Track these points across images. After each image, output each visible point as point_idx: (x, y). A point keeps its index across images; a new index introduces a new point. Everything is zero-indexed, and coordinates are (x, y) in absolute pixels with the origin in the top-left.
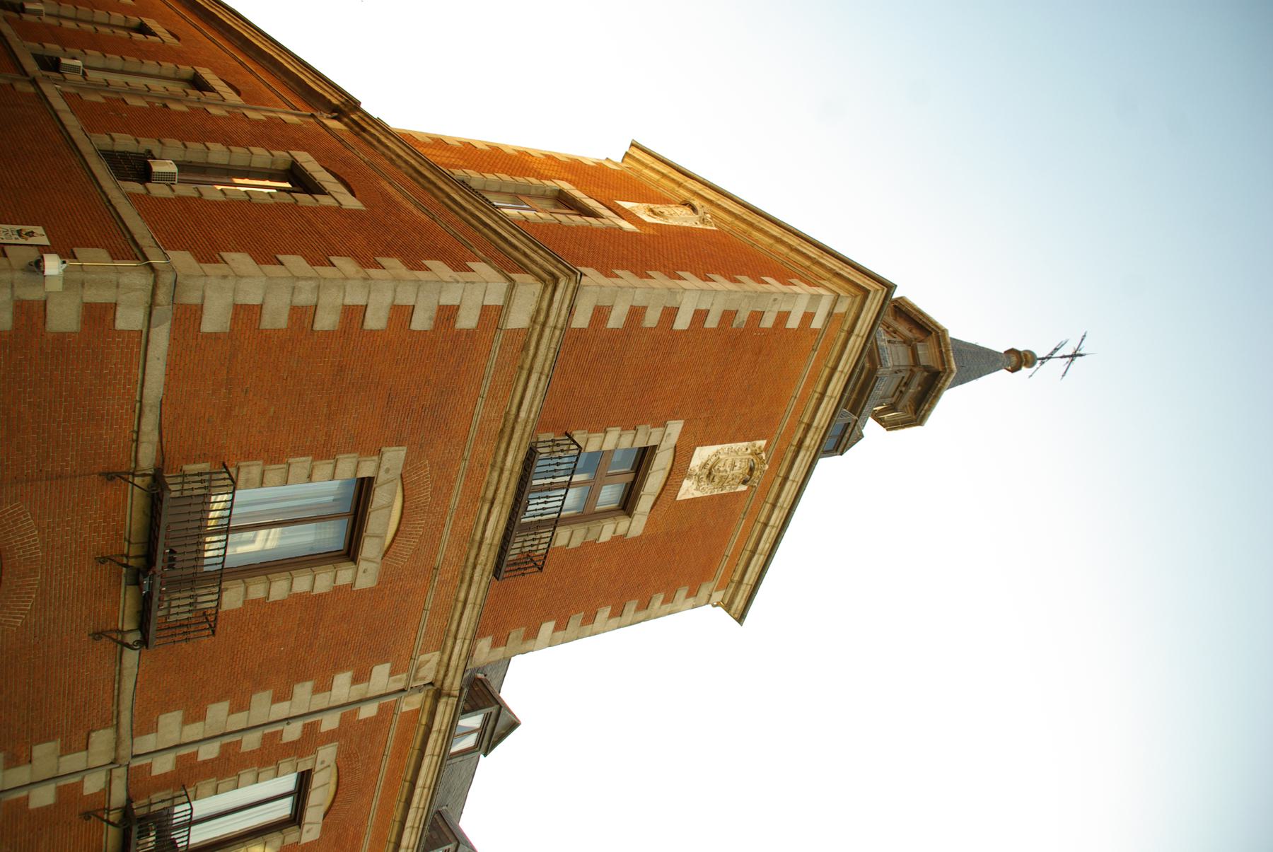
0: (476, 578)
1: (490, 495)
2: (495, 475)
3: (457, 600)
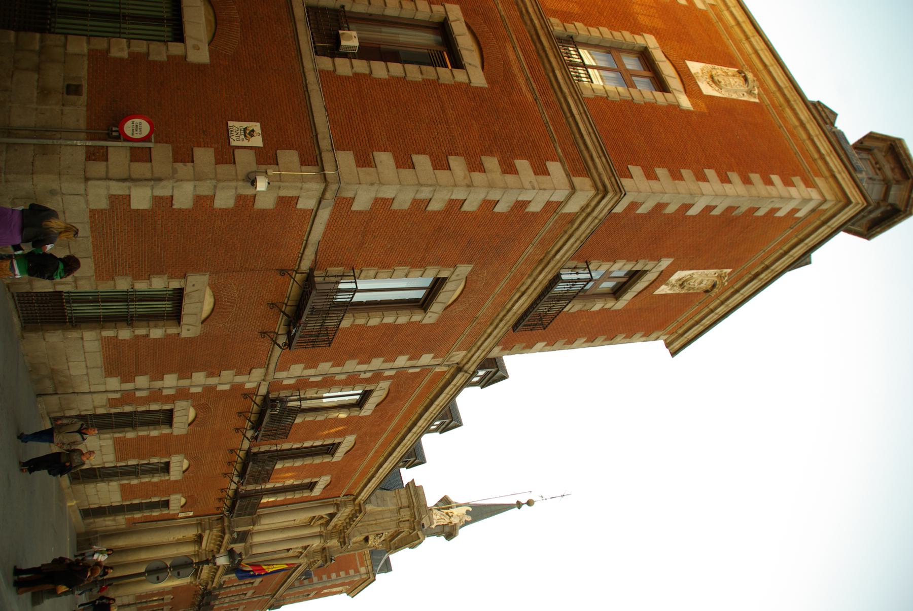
0: (501, 325)
1: (523, 289)
2: (529, 281)
3: (485, 332)
